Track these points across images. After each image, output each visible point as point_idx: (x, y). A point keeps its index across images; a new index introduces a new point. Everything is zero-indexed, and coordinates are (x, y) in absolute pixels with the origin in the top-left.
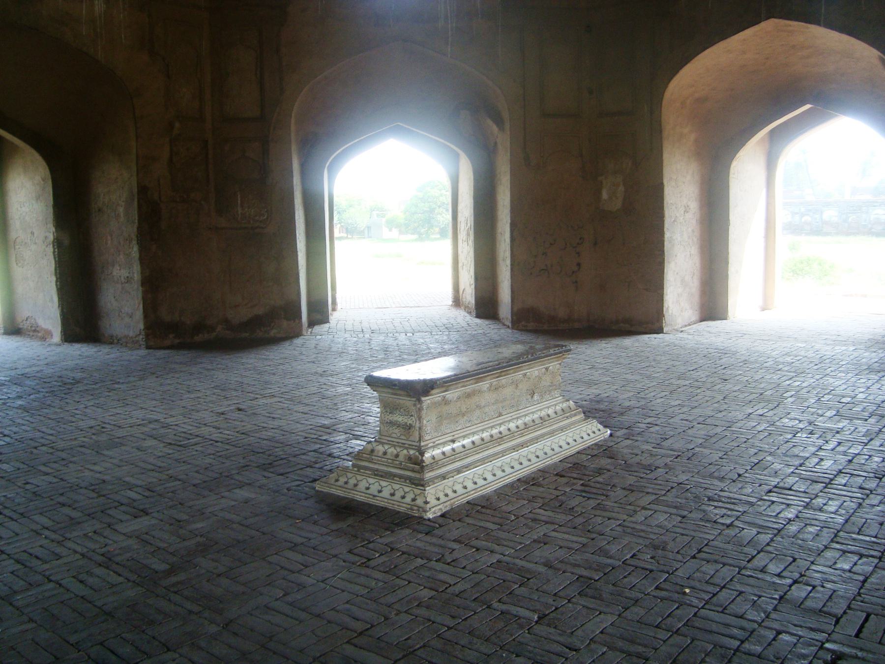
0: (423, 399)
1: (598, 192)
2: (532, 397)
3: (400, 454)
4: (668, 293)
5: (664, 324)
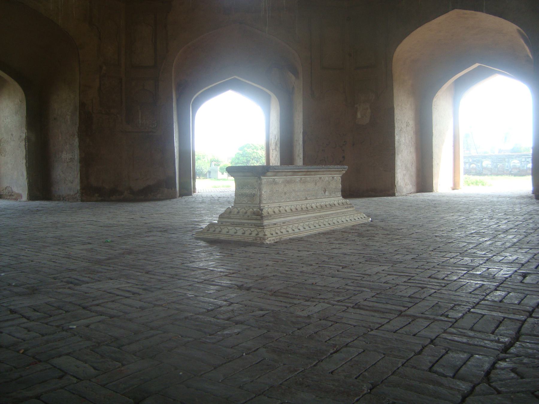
0: (262, 177)
2: (325, 193)
3: (248, 212)
4: (398, 172)
5: (396, 191)
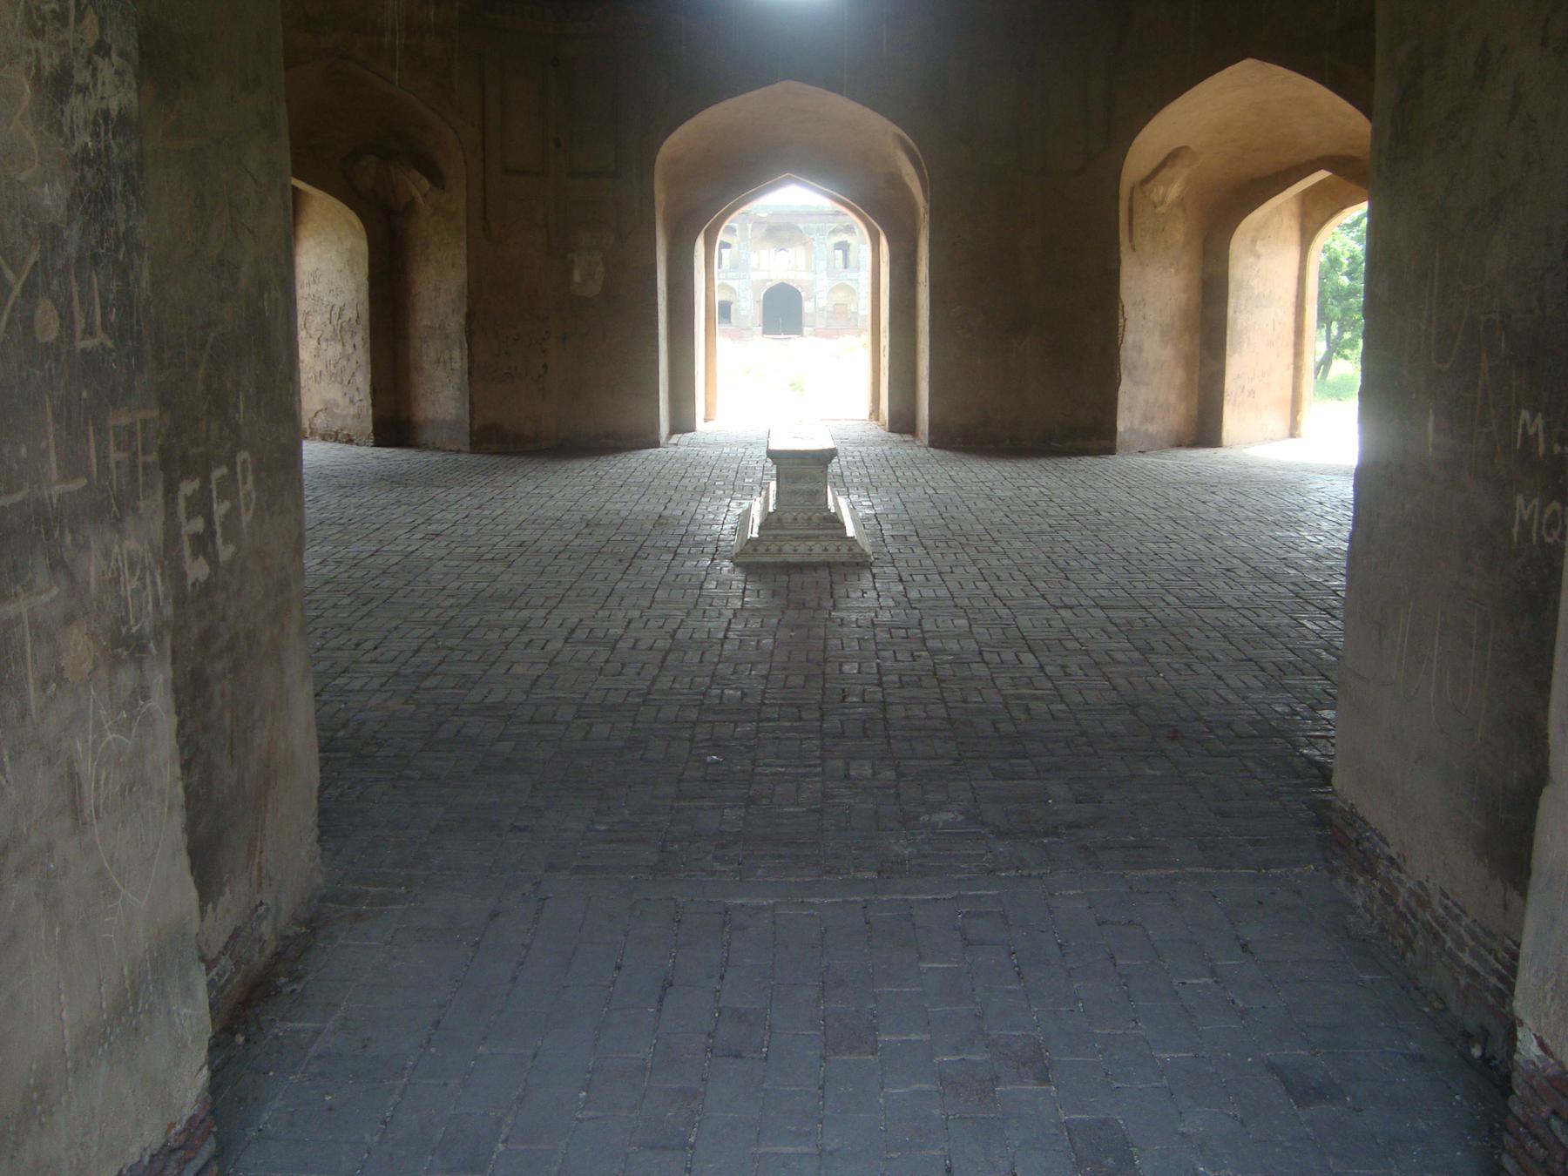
3: (813, 518)
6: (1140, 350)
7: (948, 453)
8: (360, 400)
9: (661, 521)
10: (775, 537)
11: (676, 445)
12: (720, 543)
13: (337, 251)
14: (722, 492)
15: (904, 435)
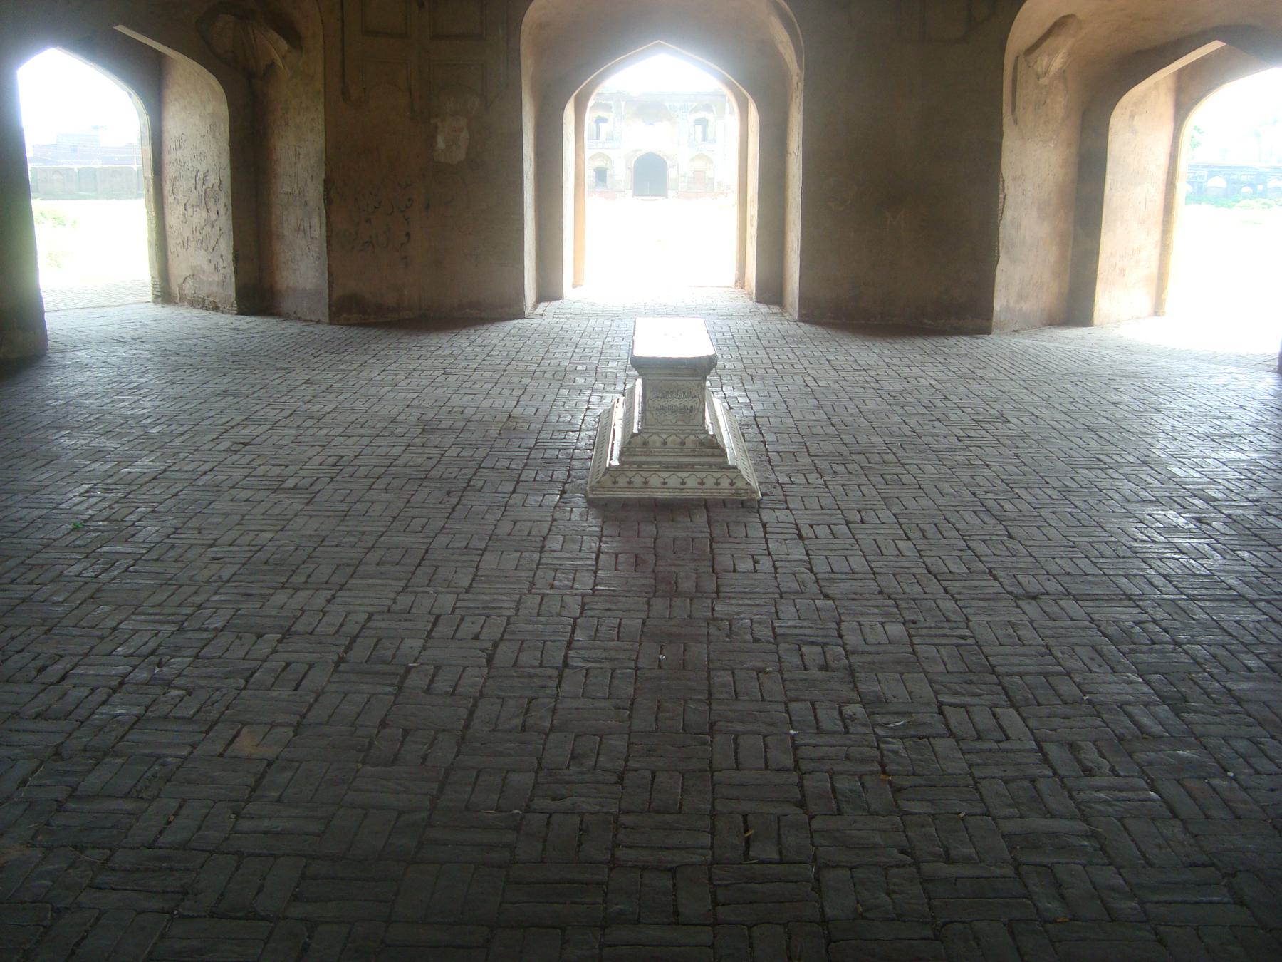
1: (431, 139)
3: (687, 441)
6: (1018, 227)
7: (820, 329)
8: (224, 267)
9: (510, 425)
10: (639, 467)
11: (541, 315)
12: (574, 463)
13: (200, 116)
14: (583, 381)
15: (771, 307)
